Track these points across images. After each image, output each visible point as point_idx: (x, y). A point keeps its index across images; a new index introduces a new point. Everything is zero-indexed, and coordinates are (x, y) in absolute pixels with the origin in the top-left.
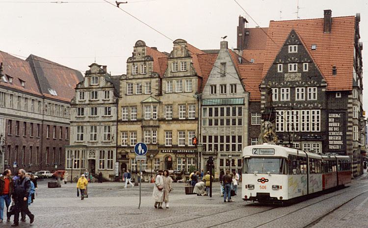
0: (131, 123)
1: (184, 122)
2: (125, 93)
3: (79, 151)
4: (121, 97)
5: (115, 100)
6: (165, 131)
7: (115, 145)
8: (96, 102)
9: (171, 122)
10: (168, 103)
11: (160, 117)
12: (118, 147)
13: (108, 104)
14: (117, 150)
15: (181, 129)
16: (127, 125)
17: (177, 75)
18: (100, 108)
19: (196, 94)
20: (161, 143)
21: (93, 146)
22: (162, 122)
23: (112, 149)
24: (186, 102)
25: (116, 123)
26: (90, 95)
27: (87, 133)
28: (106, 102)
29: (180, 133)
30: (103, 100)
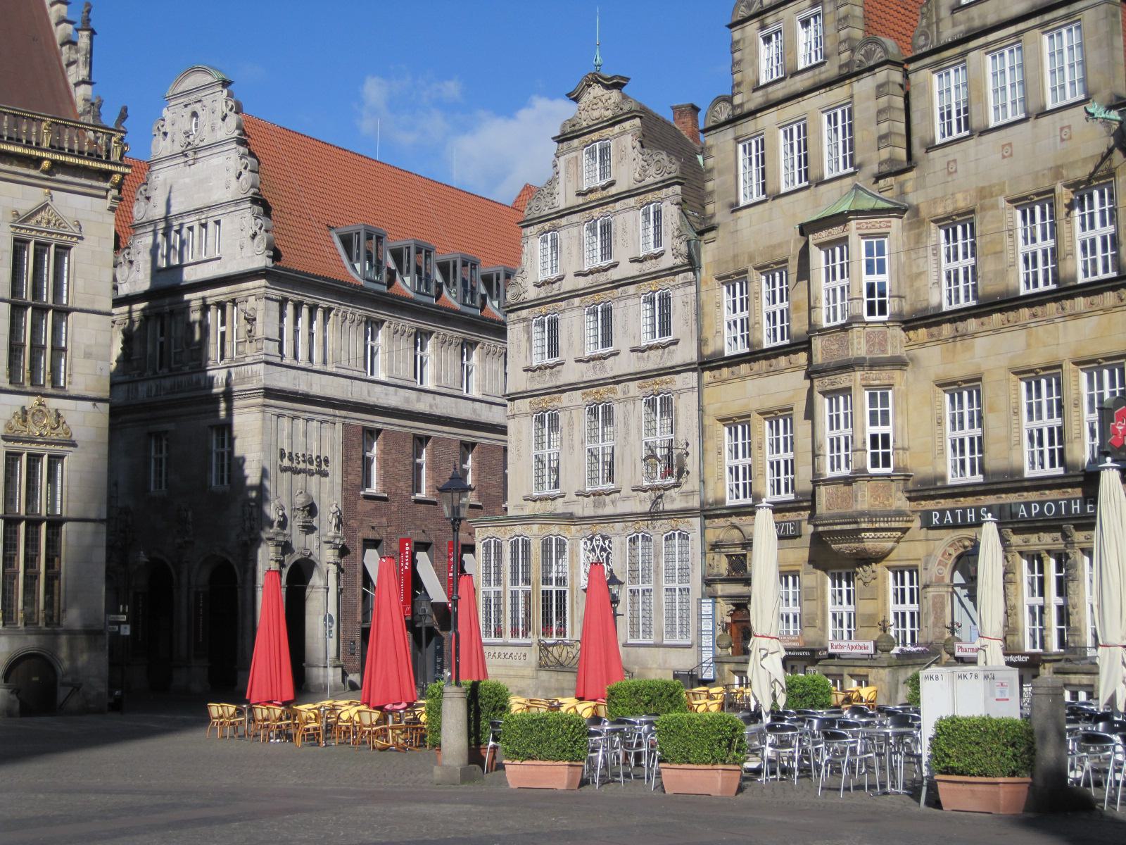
0: (764, 364)
1: (1052, 307)
2: (733, 200)
3: (526, 545)
4: (713, 228)
5: (684, 249)
6: (942, 385)
7: (695, 503)
8: (602, 278)
9: (972, 324)
10: (950, 209)
11: (906, 308)
12: (709, 512)
13: (655, 276)
14: (703, 529)
15: (1037, 359)
16: (742, 378)
17: (991, 19)
18: (622, 304)
19: (1110, 108)
20: (922, 468)
21: (601, 512)
22: (922, 332)
23: (682, 525)
24: (1057, 171)
25: (695, 374)
26: (581, 245)
27: (572, 447)
28: (649, 266)
29: (1033, 389)
30: (633, 261)
